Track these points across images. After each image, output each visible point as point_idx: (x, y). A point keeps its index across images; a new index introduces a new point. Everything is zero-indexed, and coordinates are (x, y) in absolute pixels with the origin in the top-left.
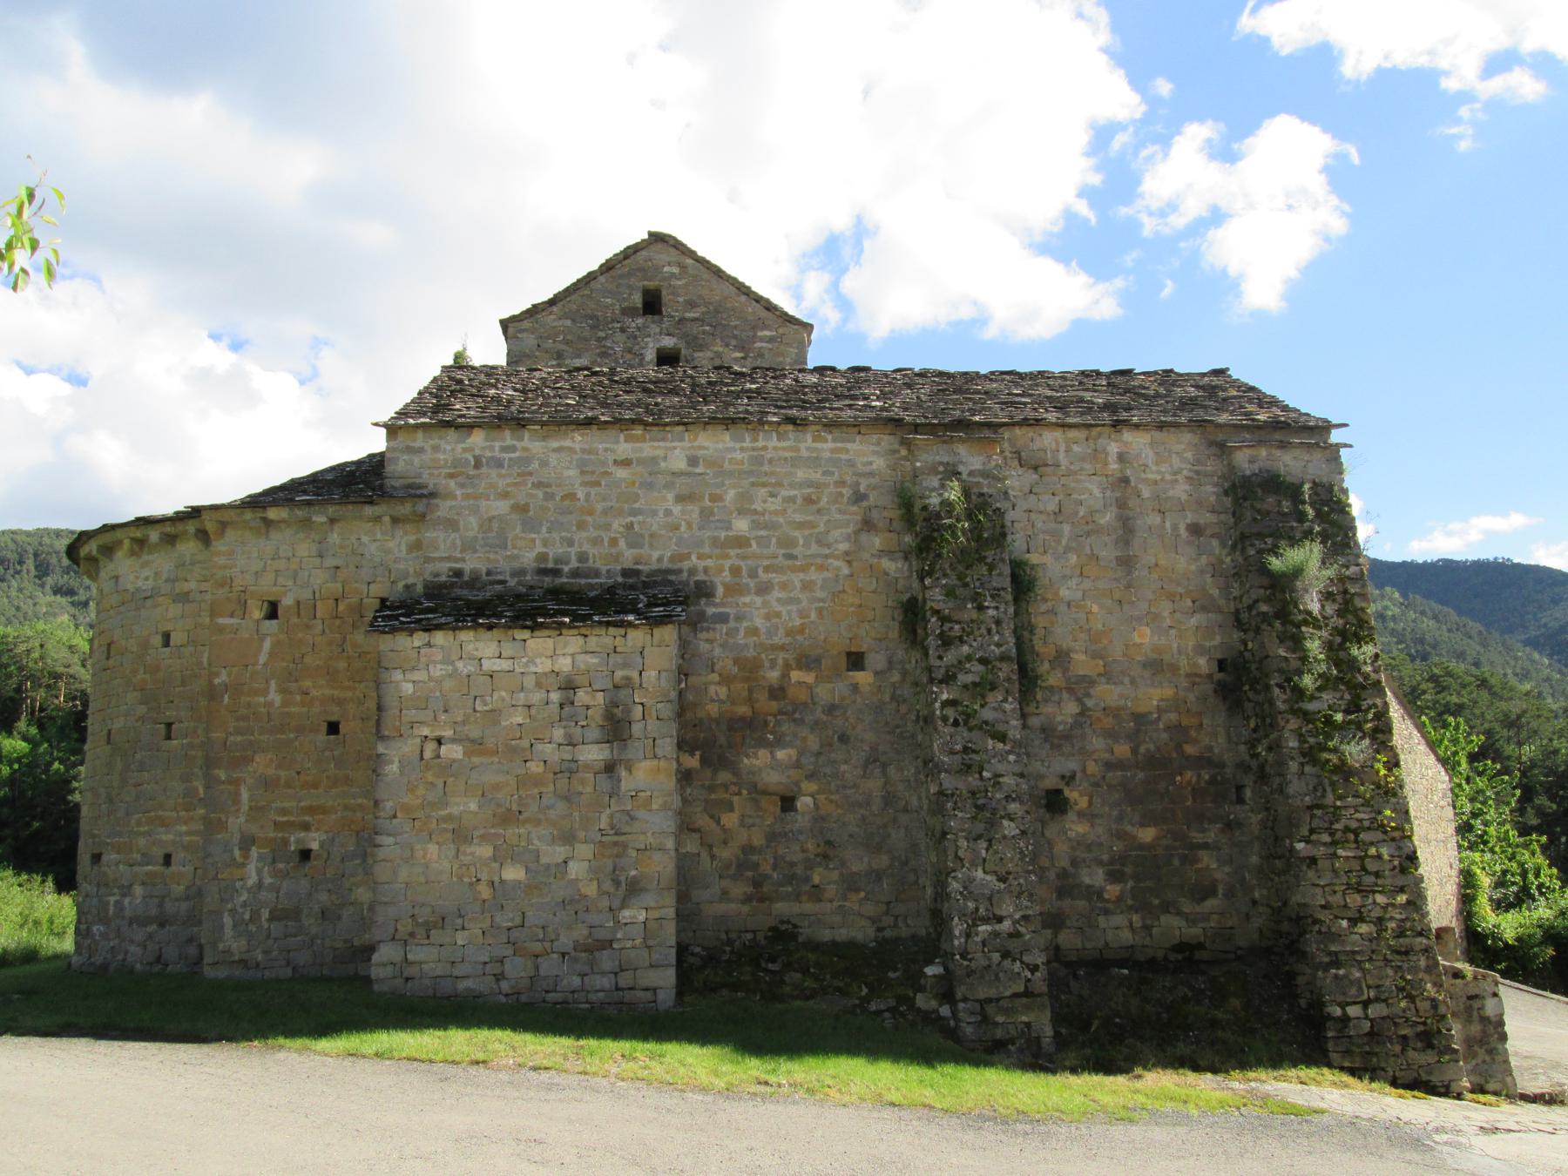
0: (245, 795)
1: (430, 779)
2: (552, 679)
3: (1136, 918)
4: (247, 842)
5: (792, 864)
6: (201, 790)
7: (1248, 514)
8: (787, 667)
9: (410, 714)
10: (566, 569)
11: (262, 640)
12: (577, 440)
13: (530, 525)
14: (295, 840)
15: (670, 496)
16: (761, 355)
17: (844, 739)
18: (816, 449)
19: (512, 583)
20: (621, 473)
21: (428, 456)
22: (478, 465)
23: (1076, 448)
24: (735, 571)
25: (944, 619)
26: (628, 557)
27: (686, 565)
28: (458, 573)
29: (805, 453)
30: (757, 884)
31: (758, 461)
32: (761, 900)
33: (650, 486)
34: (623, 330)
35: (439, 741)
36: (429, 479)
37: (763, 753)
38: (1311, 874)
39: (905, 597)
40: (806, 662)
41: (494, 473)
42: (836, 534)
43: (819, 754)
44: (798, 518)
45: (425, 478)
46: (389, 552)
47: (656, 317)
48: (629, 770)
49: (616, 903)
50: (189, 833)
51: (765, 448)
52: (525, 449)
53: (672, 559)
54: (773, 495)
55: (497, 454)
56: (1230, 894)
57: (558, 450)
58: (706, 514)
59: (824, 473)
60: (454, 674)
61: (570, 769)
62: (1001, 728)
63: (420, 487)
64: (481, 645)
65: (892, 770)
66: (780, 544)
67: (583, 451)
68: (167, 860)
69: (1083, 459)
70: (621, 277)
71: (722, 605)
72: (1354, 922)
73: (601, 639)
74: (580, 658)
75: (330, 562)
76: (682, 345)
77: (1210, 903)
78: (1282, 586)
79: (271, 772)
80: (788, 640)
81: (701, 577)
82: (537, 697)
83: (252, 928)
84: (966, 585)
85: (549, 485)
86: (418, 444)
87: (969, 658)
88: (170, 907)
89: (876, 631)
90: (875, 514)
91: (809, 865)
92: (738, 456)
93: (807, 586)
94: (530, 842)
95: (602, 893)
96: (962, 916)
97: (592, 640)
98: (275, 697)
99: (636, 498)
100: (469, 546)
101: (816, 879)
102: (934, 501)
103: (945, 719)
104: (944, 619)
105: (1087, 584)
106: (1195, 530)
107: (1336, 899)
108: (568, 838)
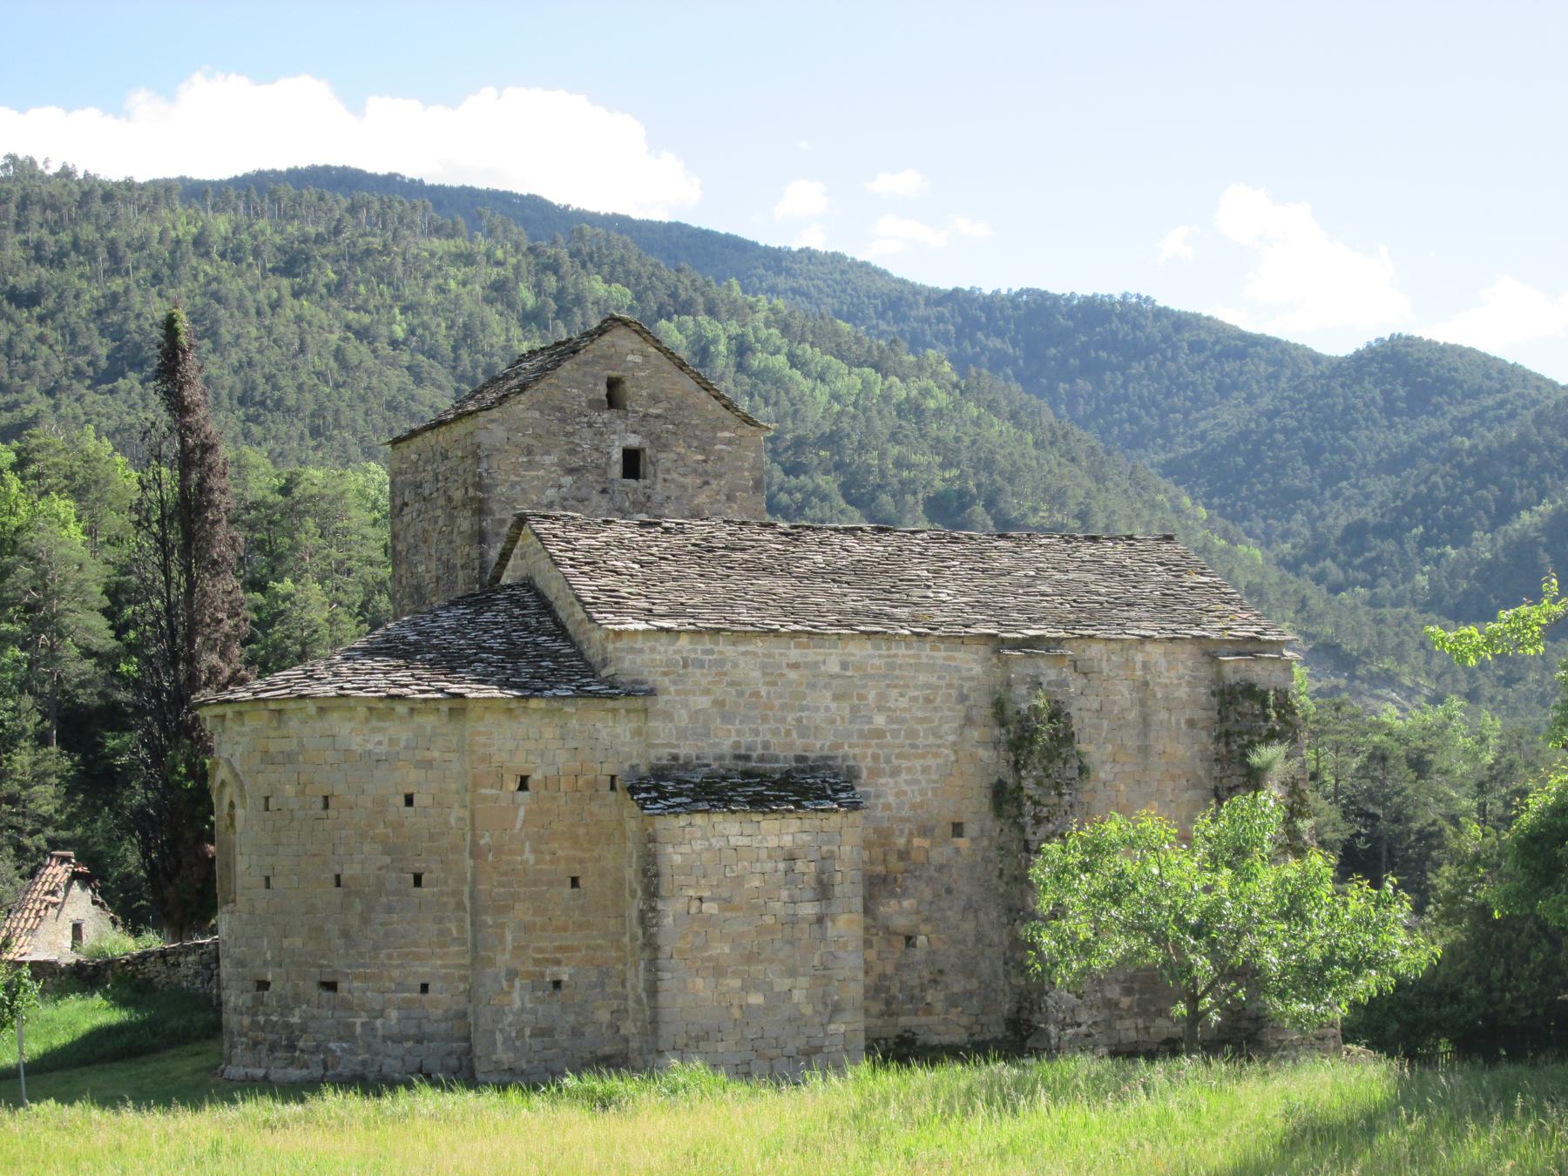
0: (509, 937)
2: (779, 852)
3: (1140, 1021)
4: (512, 975)
5: (913, 988)
7: (1233, 716)
8: (911, 835)
10: (754, 755)
11: (517, 809)
12: (758, 646)
13: (727, 718)
15: (828, 695)
16: (721, 459)
17: (949, 891)
18: (932, 657)
19: (715, 766)
20: (793, 675)
21: (646, 656)
22: (685, 666)
23: (1114, 658)
24: (875, 757)
25: (1036, 803)
26: (799, 744)
27: (841, 752)
28: (675, 758)
29: (925, 661)
30: (888, 1003)
31: (891, 666)
32: (891, 1015)
33: (813, 686)
34: (590, 425)
35: (700, 899)
36: (654, 678)
37: (893, 902)
39: (995, 780)
40: (925, 831)
41: (698, 672)
42: (946, 728)
43: (931, 903)
44: (920, 715)
45: (645, 676)
46: (616, 736)
47: (621, 412)
48: (833, 921)
49: (826, 1019)
50: (443, 967)
51: (896, 656)
52: (720, 652)
54: (902, 695)
55: (700, 656)
57: (744, 654)
58: (854, 710)
59: (939, 677)
60: (710, 848)
61: (793, 921)
63: (642, 683)
64: (728, 825)
65: (981, 915)
66: (907, 736)
68: (425, 988)
70: (586, 363)
71: (866, 785)
73: (812, 822)
75: (571, 744)
76: (646, 445)
79: (529, 918)
81: (851, 762)
82: (769, 866)
83: (518, 1043)
84: (1049, 776)
85: (739, 684)
86: (639, 645)
89: (975, 807)
90: (975, 712)
91: (923, 989)
92: (877, 661)
93: (925, 770)
94: (766, 975)
95: (816, 1012)
97: (807, 822)
98: (529, 856)
99: (804, 696)
100: (682, 734)
101: (929, 999)
102: (1024, 706)
104: (1036, 803)
105: (1117, 769)
106: (1191, 723)
108: (792, 973)
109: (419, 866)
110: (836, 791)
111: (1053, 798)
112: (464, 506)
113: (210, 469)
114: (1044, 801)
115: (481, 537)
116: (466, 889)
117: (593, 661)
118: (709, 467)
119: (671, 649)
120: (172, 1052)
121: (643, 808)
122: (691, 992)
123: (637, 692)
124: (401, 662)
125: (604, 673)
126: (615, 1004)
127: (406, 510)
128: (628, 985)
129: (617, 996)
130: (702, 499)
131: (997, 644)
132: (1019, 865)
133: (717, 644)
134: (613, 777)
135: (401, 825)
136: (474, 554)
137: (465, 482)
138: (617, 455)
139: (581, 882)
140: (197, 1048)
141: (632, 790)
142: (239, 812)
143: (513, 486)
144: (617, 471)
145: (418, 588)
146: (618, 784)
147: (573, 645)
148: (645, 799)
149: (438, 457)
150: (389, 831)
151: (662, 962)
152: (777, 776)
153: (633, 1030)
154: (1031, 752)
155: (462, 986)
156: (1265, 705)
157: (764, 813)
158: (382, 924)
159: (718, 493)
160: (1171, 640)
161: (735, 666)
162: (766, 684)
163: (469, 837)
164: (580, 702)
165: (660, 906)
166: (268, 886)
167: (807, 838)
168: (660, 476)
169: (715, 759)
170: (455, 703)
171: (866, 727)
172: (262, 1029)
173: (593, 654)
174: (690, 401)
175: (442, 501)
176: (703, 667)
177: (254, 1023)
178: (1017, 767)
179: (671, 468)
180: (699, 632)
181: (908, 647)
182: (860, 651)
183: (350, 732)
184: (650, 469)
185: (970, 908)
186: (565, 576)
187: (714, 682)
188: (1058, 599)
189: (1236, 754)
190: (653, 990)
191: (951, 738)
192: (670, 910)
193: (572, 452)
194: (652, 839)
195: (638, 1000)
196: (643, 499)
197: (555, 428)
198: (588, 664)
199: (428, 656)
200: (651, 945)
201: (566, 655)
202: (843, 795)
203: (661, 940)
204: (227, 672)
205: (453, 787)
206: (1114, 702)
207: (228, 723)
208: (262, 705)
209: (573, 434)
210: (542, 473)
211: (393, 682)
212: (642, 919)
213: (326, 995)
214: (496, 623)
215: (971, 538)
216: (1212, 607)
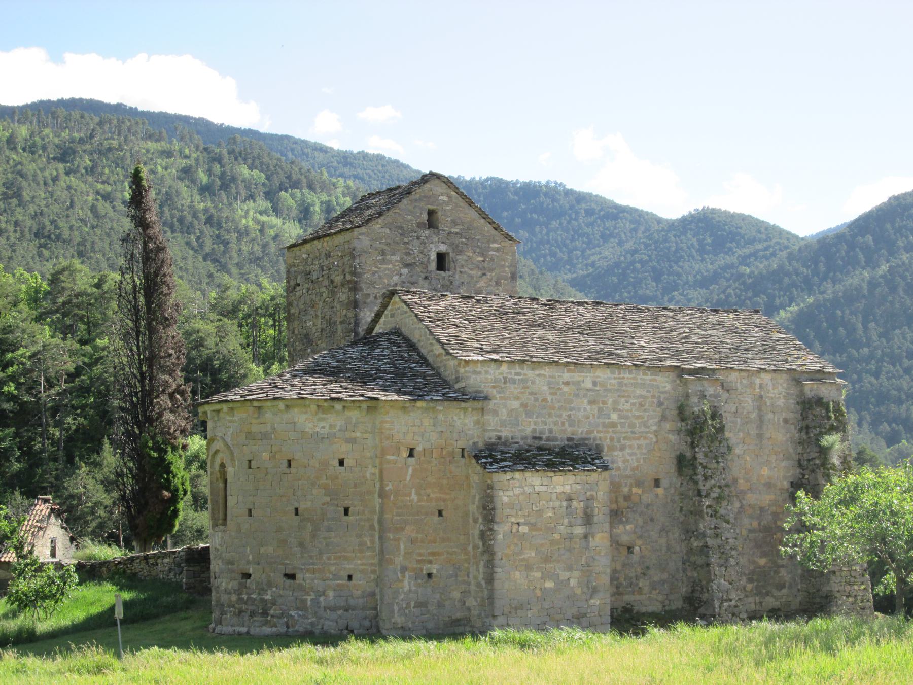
0: (402, 547)
1: (516, 541)
2: (563, 495)
3: (757, 598)
4: (404, 569)
5: (631, 578)
6: (368, 543)
7: (811, 417)
8: (631, 486)
9: (507, 511)
10: (544, 437)
12: (547, 371)
13: (529, 414)
14: (426, 569)
15: (586, 401)
16: (492, 260)
17: (652, 520)
19: (522, 443)
20: (566, 389)
21: (483, 376)
22: (505, 383)
23: (744, 381)
24: (612, 439)
25: (705, 467)
26: (569, 430)
27: (592, 436)
28: (499, 438)
29: (639, 381)
30: (617, 587)
32: (619, 594)
33: (577, 395)
34: (418, 238)
35: (518, 524)
37: (621, 527)
38: (834, 578)
39: (678, 453)
40: (639, 484)
41: (512, 386)
42: (651, 421)
43: (642, 527)
44: (637, 413)
45: (482, 388)
46: (465, 425)
47: (436, 231)
48: (593, 537)
49: (589, 596)
50: (362, 565)
51: (623, 378)
52: (525, 375)
53: (587, 432)
54: (627, 402)
55: (513, 377)
56: (790, 586)
57: (539, 375)
59: (648, 391)
60: (524, 493)
61: (570, 537)
62: (727, 517)
63: (480, 392)
64: (534, 479)
65: (670, 534)
66: (629, 426)
67: (550, 376)
68: (350, 578)
69: (746, 387)
70: (416, 200)
71: (607, 455)
72: (847, 597)
73: (582, 477)
74: (574, 486)
75: (439, 429)
76: (450, 251)
77: (785, 591)
78: (824, 452)
79: (414, 535)
80: (631, 473)
81: (598, 442)
82: (557, 504)
83: (407, 611)
84: (711, 451)
85: (536, 394)
86: (478, 370)
87: (714, 486)
88: (352, 602)
89: (667, 471)
90: (667, 412)
91: (637, 578)
92: (613, 381)
93: (639, 447)
94: (555, 570)
95: (583, 593)
96: (718, 599)
97: (578, 477)
98: (414, 497)
99: (571, 402)
100: (503, 424)
101: (641, 585)
102: (696, 409)
103: (707, 514)
104: (705, 467)
106: (786, 421)
107: (841, 588)
108: (570, 568)
109: (347, 503)
110: (593, 459)
111: (713, 465)
112: (343, 285)
113: (163, 262)
114: (709, 466)
115: (355, 304)
116: (376, 517)
117: (448, 379)
118: (486, 265)
119: (497, 372)
120: (167, 618)
121: (485, 468)
122: (513, 580)
123: (478, 398)
124: (331, 378)
125: (457, 386)
126: (463, 587)
127: (298, 288)
128: (471, 576)
129: (464, 582)
130: (481, 284)
131: (680, 372)
132: (694, 503)
133: (523, 369)
134: (463, 449)
135: (337, 478)
136: (350, 314)
137: (344, 271)
138: (433, 256)
139: (444, 513)
140: (182, 614)
141: (477, 457)
142: (230, 470)
143: (374, 273)
144: (433, 266)
145: (307, 336)
146: (466, 454)
147: (433, 369)
148: (486, 463)
149: (323, 255)
150: (330, 482)
151: (497, 562)
152: (557, 450)
153: (475, 603)
154: (701, 437)
155: (373, 576)
156: (828, 410)
157: (555, 472)
158: (325, 538)
159: (491, 280)
160: (774, 371)
161: (533, 382)
162: (551, 394)
163: (378, 485)
164: (446, 403)
165: (496, 528)
166: (250, 515)
167: (578, 487)
168: (458, 269)
169: (522, 439)
170: (370, 403)
171: (607, 421)
172: (246, 603)
173: (449, 374)
174: (475, 225)
175: (326, 283)
176: (515, 383)
177: (240, 600)
178: (693, 445)
179: (465, 264)
180: (513, 362)
181: (630, 373)
182: (603, 375)
183: (305, 420)
184: (452, 265)
185: (664, 530)
186: (427, 327)
187: (522, 393)
188: (706, 346)
189: (813, 439)
190: (490, 579)
191: (654, 428)
192: (501, 530)
193: (408, 254)
194: (490, 487)
195: (479, 585)
196: (448, 283)
197: (398, 239)
198: (445, 381)
199: (348, 375)
200: (489, 551)
201: (428, 375)
202: (597, 461)
203: (496, 549)
204: (174, 386)
205: (368, 454)
206: (744, 408)
207: (221, 415)
208: (248, 403)
209: (408, 243)
210: (390, 266)
211: (331, 390)
212: (482, 535)
213: (289, 582)
214: (384, 356)
215: (648, 309)
216: (791, 352)
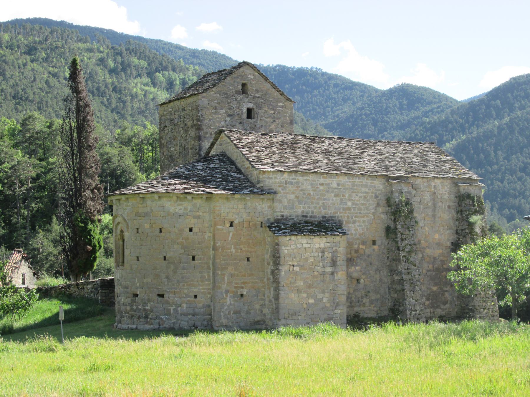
0: (226, 278)
2: (319, 250)
3: (432, 310)
4: (227, 292)
5: (359, 298)
7: (463, 205)
8: (359, 244)
10: (309, 215)
11: (229, 233)
12: (310, 177)
13: (300, 202)
15: (333, 195)
16: (279, 113)
17: (371, 264)
18: (367, 182)
19: (296, 219)
20: (321, 188)
21: (273, 180)
22: (286, 184)
23: (425, 184)
24: (348, 217)
25: (402, 234)
26: (323, 212)
28: (283, 216)
29: (364, 184)
30: (351, 303)
31: (353, 185)
33: (328, 192)
34: (236, 100)
35: (293, 266)
36: (276, 188)
37: (353, 268)
39: (386, 225)
40: (363, 243)
41: (290, 186)
42: (371, 207)
43: (365, 268)
44: (363, 202)
45: (273, 187)
46: (263, 208)
48: (337, 274)
49: (334, 308)
50: (202, 289)
51: (355, 182)
52: (298, 179)
54: (357, 196)
56: (451, 303)
57: (306, 180)
58: (341, 200)
59: (369, 189)
60: (297, 248)
61: (324, 274)
62: (414, 263)
63: (272, 189)
67: (312, 181)
68: (196, 296)
69: (426, 187)
70: (235, 78)
71: (345, 226)
72: (484, 309)
73: (330, 239)
75: (248, 211)
76: (255, 107)
77: (448, 305)
78: (471, 225)
79: (233, 272)
81: (340, 219)
82: (316, 254)
83: (228, 316)
84: (405, 224)
86: (271, 176)
87: (407, 244)
88: (197, 311)
89: (380, 235)
90: (380, 202)
92: (349, 183)
93: (364, 222)
94: (315, 293)
95: (331, 306)
96: (409, 310)
97: (328, 239)
98: (233, 250)
100: (285, 208)
101: (364, 301)
102: (397, 200)
103: (403, 260)
104: (402, 234)
105: (425, 222)
106: (449, 207)
107: (480, 304)
108: (323, 292)
109: (194, 253)
110: (337, 229)
111: (407, 232)
112: (192, 127)
113: (88, 113)
114: (404, 233)
115: (199, 138)
116: (211, 262)
117: (253, 181)
118: (275, 115)
119: (282, 178)
120: (90, 319)
121: (274, 233)
122: (290, 298)
124: (185, 181)
125: (258, 186)
126: (261, 302)
127: (166, 129)
128: (266, 296)
129: (262, 299)
130: (273, 126)
131: (388, 178)
132: (395, 255)
133: (297, 176)
134: (262, 222)
135: (188, 239)
136: (197, 144)
137: (193, 118)
138: (245, 110)
139: (250, 259)
140: (98, 318)
141: (270, 227)
142: (126, 234)
143: (210, 120)
144: (245, 116)
145: (171, 156)
146: (263, 226)
147: (244, 176)
148: (275, 230)
149: (181, 109)
150: (184, 241)
151: (281, 288)
152: (316, 223)
153: (268, 312)
154: (400, 216)
155: (209, 296)
156: (473, 201)
157: (315, 236)
158: (181, 274)
159: (278, 124)
160: (443, 178)
161: (303, 184)
162: (313, 190)
163: (212, 243)
164: (252, 196)
165: (280, 268)
166: (138, 260)
167: (329, 245)
168: (259, 118)
169: (296, 217)
170: (209, 195)
171: (345, 206)
172: (135, 311)
173: (253, 179)
174: (269, 92)
175: (182, 125)
176: (292, 184)
177: (132, 309)
178: (395, 221)
179: (263, 115)
180: (291, 172)
181: (359, 178)
182: (343, 180)
183: (169, 205)
184: (256, 115)
185: (378, 270)
186: (241, 151)
187: (296, 190)
188: (403, 164)
189: (465, 218)
190: (277, 298)
191: (373, 211)
192: (284, 269)
193: (230, 109)
194: (277, 244)
195: (270, 301)
196: (253, 126)
197: (224, 100)
198: (251, 183)
199: (195, 179)
200: (276, 281)
201: (242, 179)
202: (339, 230)
203: (280, 280)
204: (94, 185)
205: (207, 225)
206: (424, 199)
207: (121, 202)
208: (137, 195)
209: (230, 102)
210: (220, 116)
211: (185, 188)
212: (273, 272)
213: (160, 299)
214: (216, 168)
215: (370, 142)
216: (452, 167)
